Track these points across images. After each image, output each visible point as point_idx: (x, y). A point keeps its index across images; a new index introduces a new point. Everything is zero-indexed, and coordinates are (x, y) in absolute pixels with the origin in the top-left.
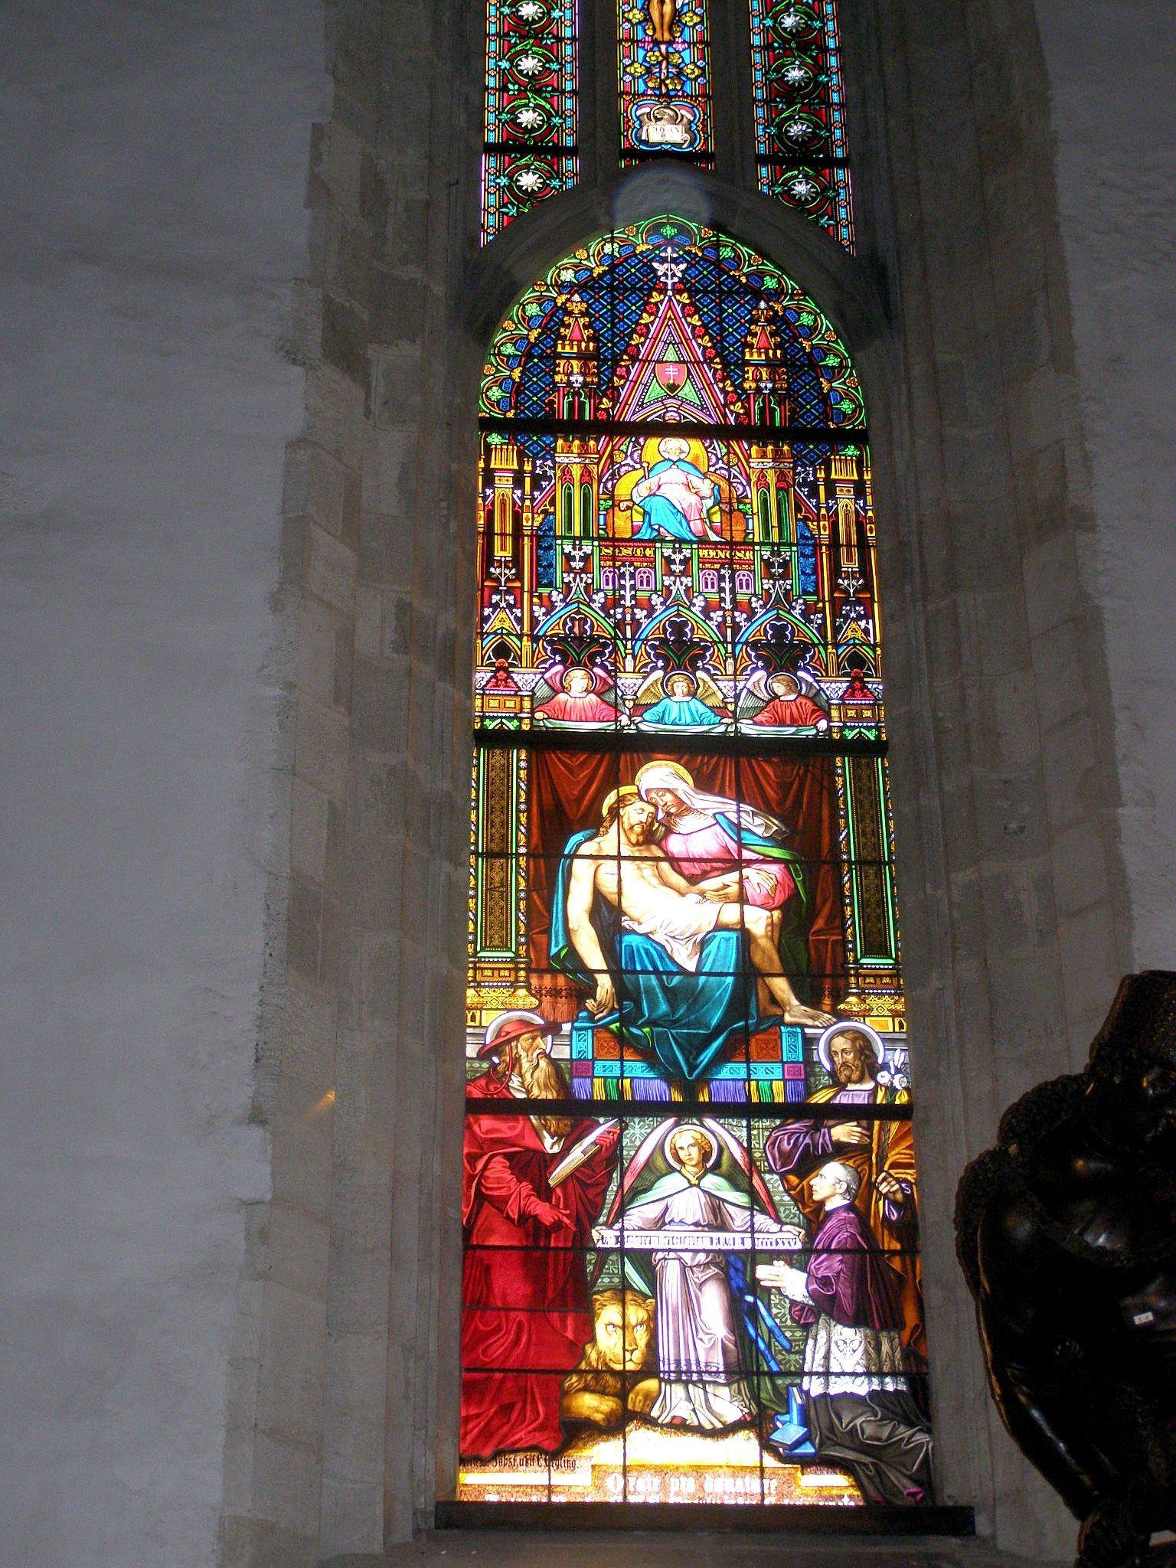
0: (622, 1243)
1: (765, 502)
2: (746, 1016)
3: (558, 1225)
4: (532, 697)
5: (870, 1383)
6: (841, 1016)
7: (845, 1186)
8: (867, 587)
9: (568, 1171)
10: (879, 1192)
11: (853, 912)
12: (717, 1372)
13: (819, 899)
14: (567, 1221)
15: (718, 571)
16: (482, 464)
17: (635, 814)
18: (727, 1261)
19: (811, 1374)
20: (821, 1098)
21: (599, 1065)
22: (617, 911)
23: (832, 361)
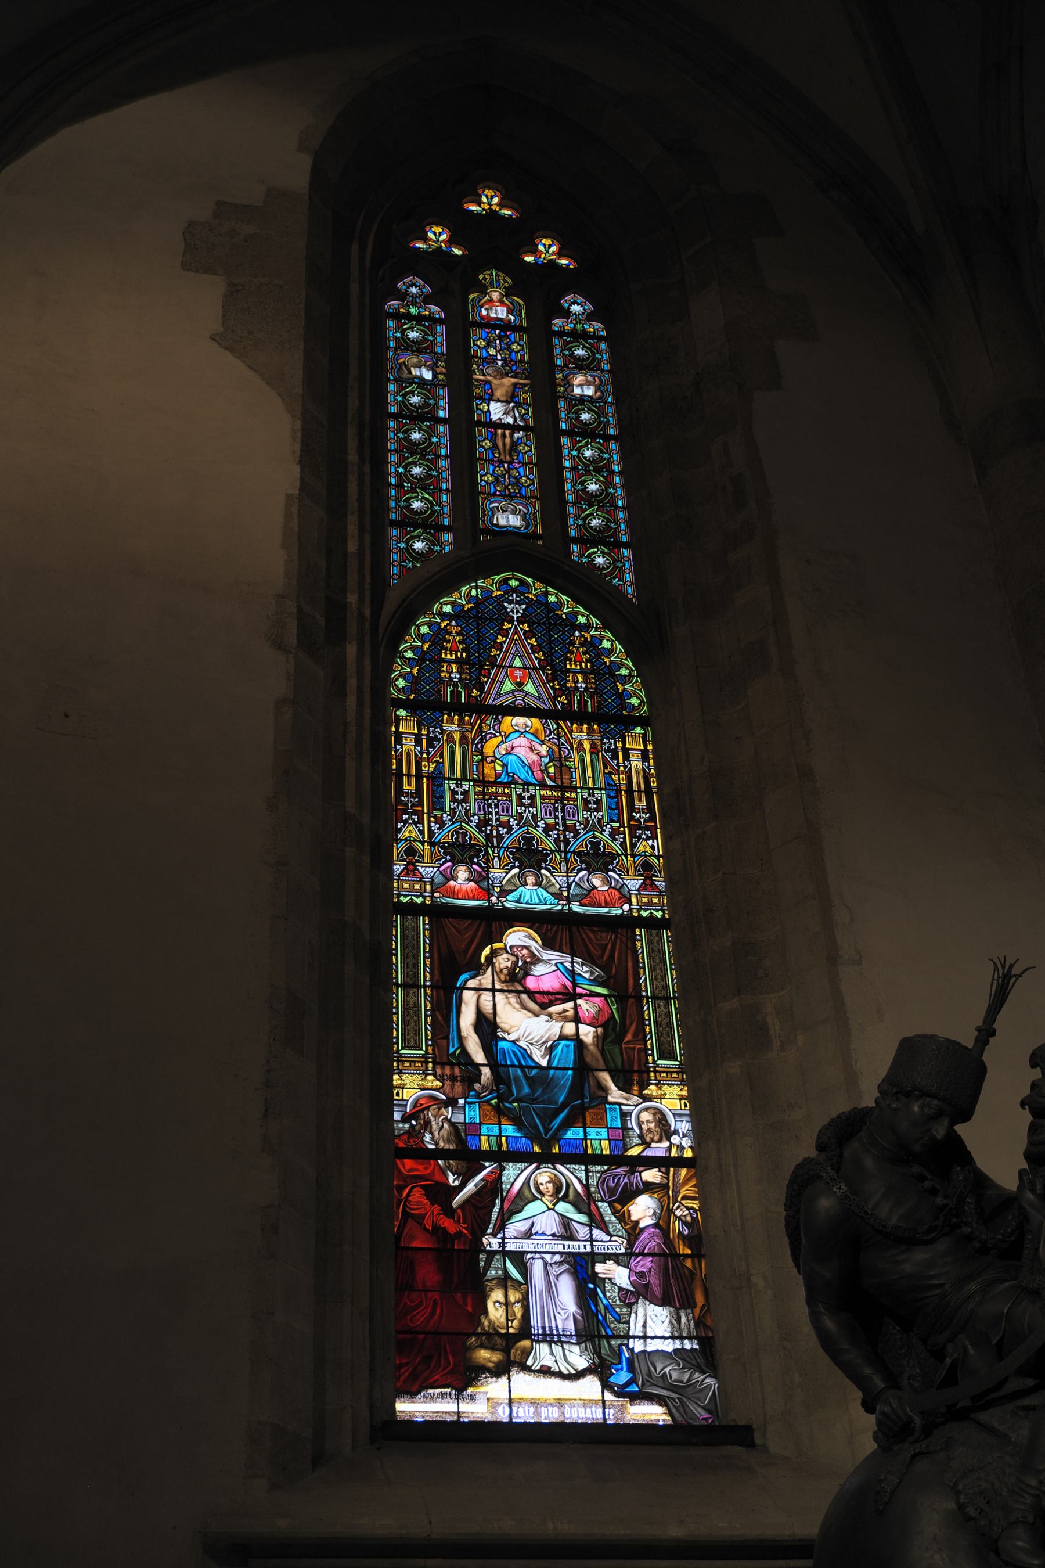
0: (504, 1247)
1: (583, 761)
2: (582, 1097)
4: (432, 882)
8: (653, 818)
9: (465, 1197)
11: (650, 1030)
12: (571, 1335)
13: (628, 1022)
15: (554, 805)
16: (393, 729)
17: (503, 962)
19: (634, 1337)
20: (634, 1152)
21: (484, 1129)
23: (624, 672)
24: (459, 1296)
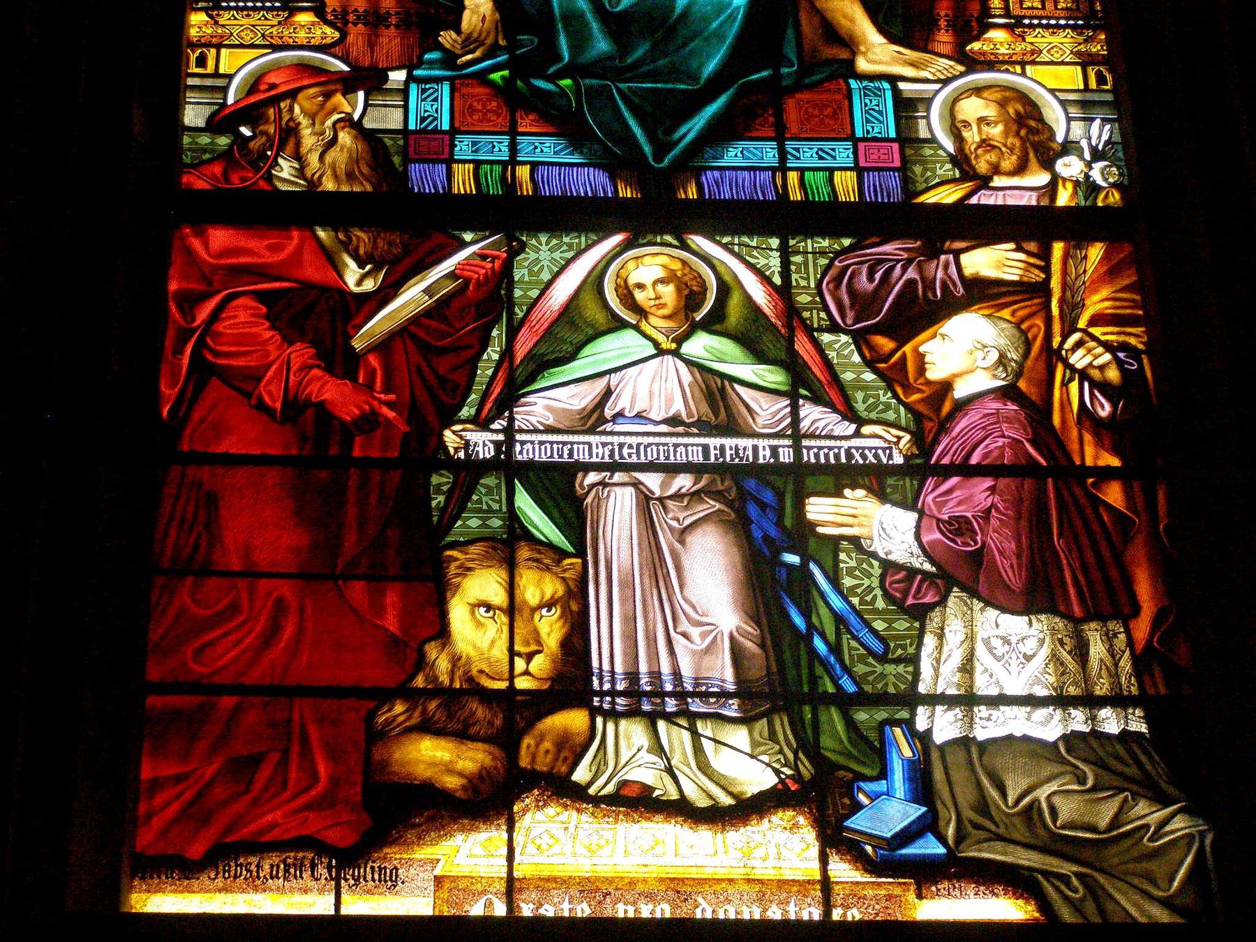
2: (777, 59)
3: (370, 421)
5: (1066, 719)
6: (973, 64)
7: (995, 355)
10: (1066, 363)
12: (724, 695)
14: (391, 414)
18: (741, 489)
19: (933, 700)
21: (463, 147)
24: (357, 591)
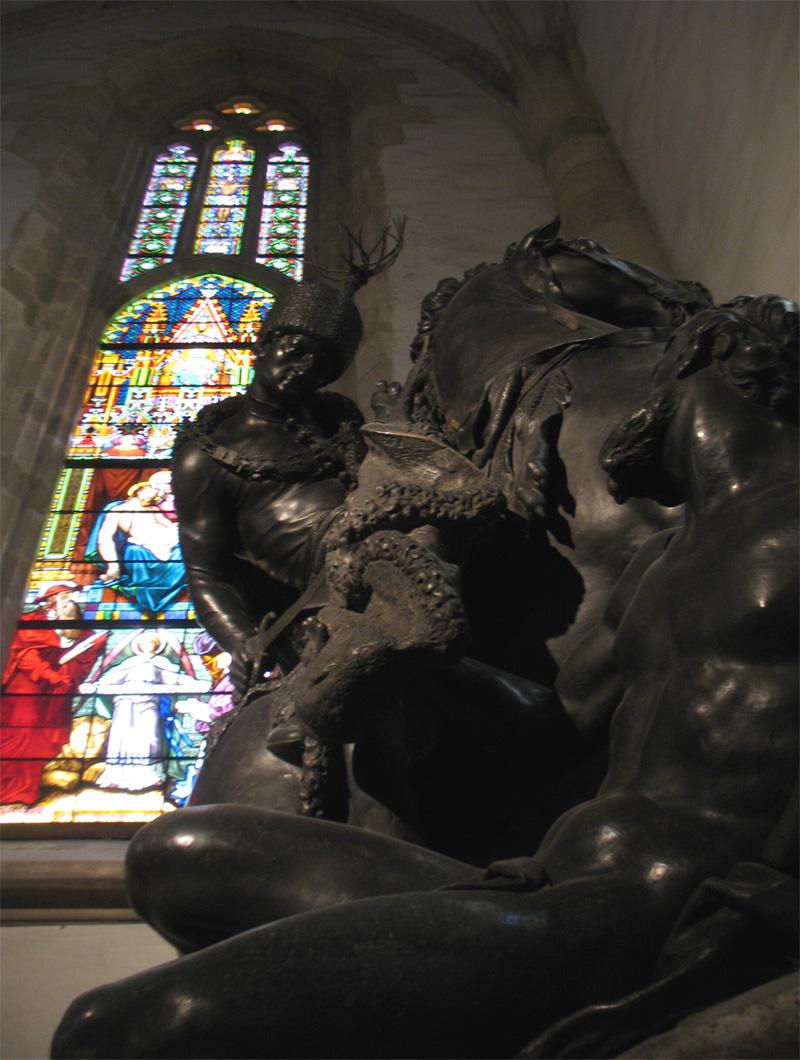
3: (60, 684)
22: (127, 535)
